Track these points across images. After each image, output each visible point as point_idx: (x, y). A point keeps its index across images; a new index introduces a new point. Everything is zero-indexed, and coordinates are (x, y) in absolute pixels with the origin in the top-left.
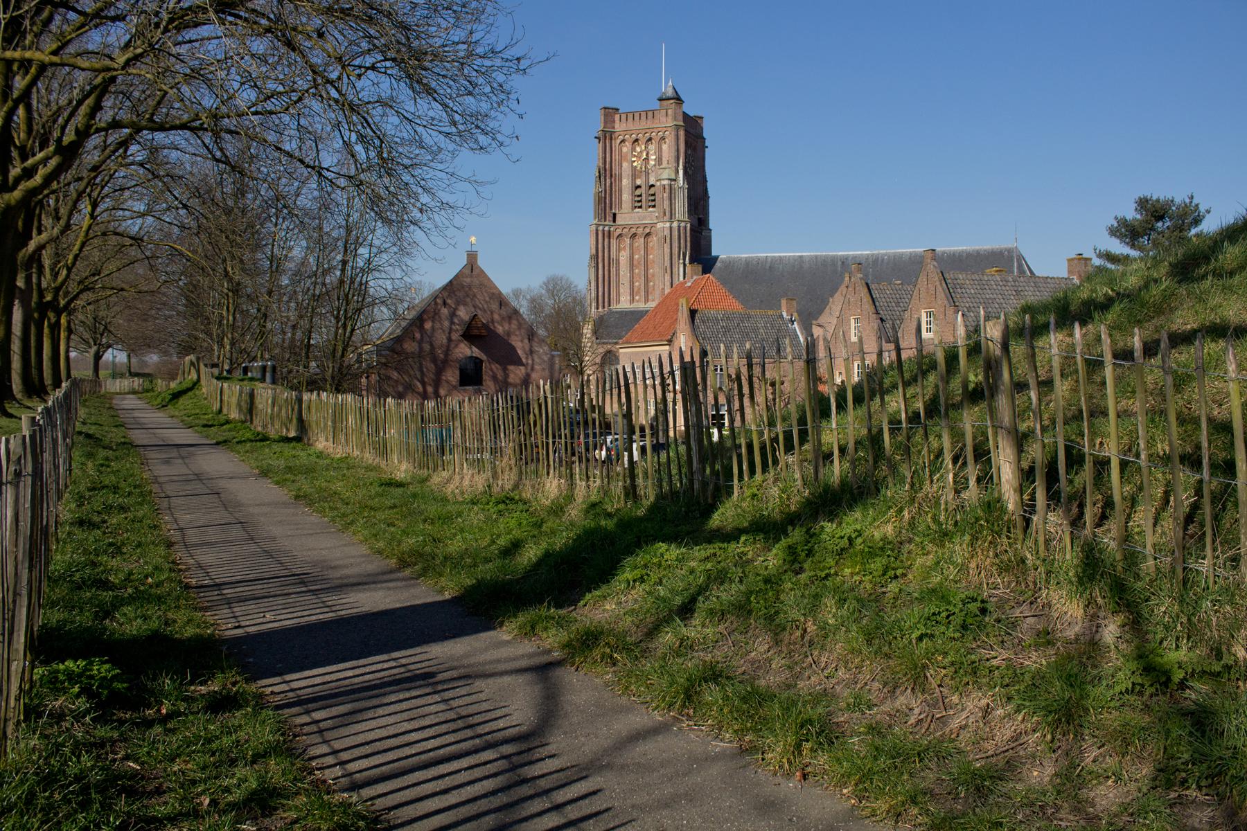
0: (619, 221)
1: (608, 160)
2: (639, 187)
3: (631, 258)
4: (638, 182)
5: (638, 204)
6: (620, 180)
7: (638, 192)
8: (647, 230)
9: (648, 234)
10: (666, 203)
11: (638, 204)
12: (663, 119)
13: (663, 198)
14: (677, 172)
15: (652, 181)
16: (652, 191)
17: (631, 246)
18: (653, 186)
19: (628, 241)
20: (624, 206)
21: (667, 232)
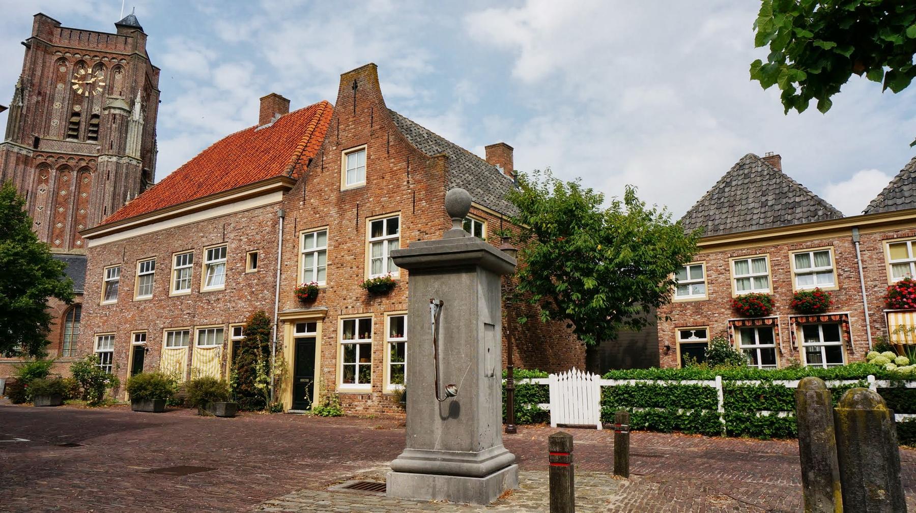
0: (43, 147)
1: (39, 73)
2: (77, 114)
3: (56, 193)
4: (77, 108)
5: (73, 131)
6: (52, 100)
7: (75, 119)
8: (83, 164)
9: (85, 169)
10: (115, 135)
11: (73, 131)
12: (121, 46)
13: (111, 132)
14: (132, 104)
15: (96, 110)
16: (95, 121)
17: (58, 179)
18: (96, 116)
19: (53, 172)
20: (53, 131)
21: (111, 168)
